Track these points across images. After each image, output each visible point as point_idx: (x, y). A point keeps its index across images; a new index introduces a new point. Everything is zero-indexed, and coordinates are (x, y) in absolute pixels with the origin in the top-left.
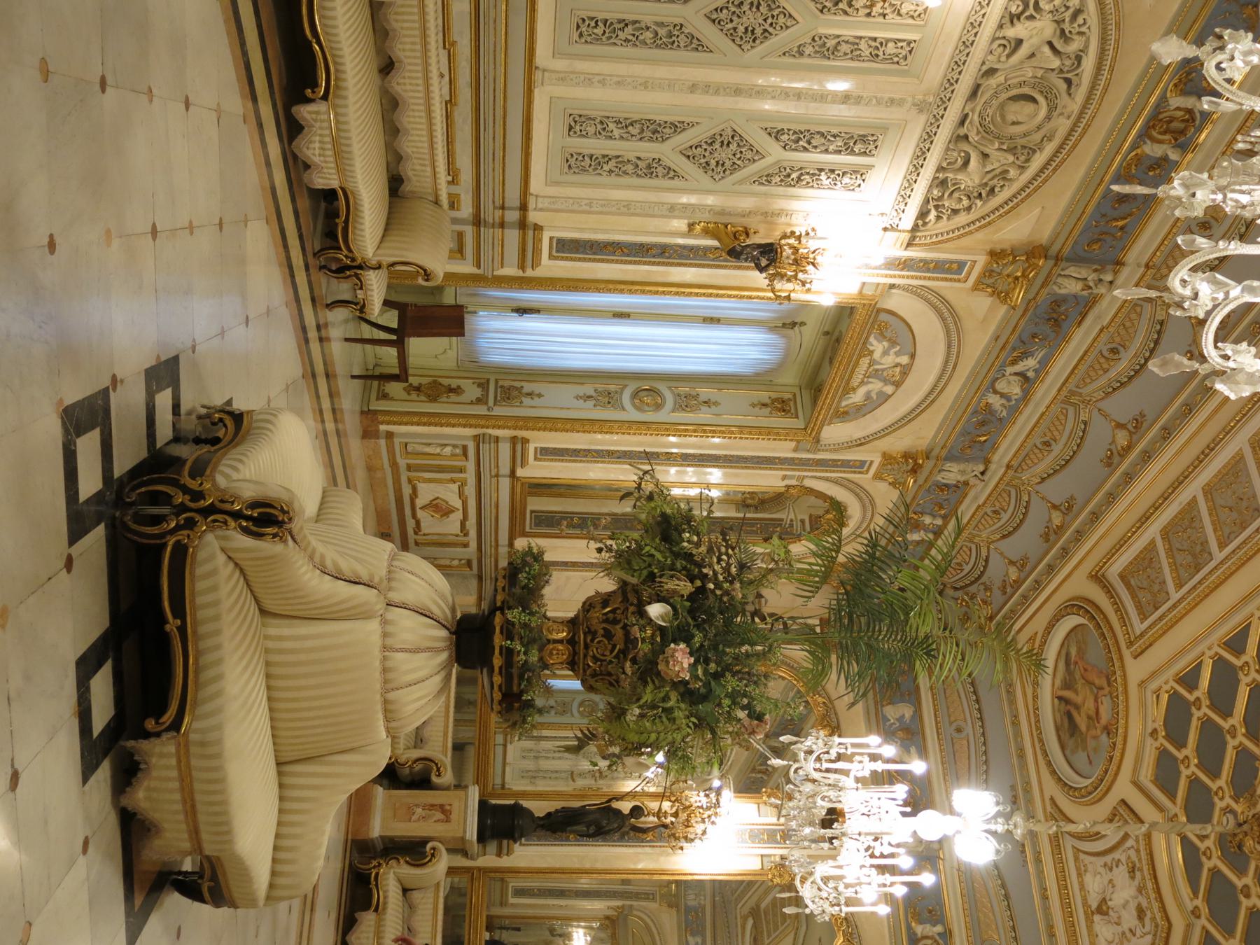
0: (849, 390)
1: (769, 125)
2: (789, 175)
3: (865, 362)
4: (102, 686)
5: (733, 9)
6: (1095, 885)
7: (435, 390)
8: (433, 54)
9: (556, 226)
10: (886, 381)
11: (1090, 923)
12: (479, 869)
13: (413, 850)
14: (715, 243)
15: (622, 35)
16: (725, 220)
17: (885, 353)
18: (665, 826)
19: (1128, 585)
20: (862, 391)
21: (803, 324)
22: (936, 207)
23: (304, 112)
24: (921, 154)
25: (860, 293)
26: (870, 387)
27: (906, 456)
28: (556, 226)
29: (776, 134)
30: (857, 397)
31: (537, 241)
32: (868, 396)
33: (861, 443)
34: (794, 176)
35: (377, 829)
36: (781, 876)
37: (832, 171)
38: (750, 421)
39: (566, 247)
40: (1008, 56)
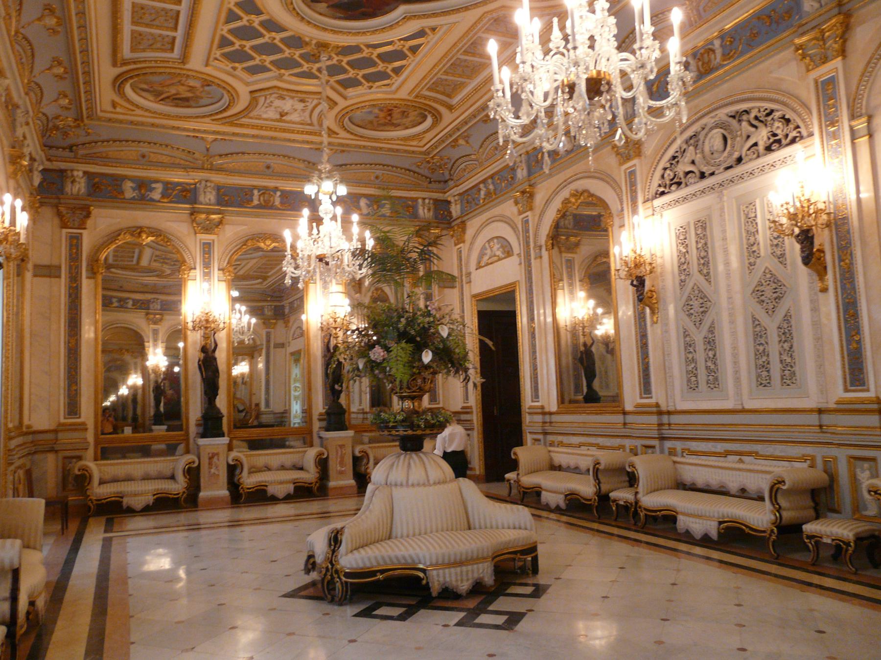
6: (272, 114)
11: (285, 122)
19: (144, 50)
35: (224, 492)
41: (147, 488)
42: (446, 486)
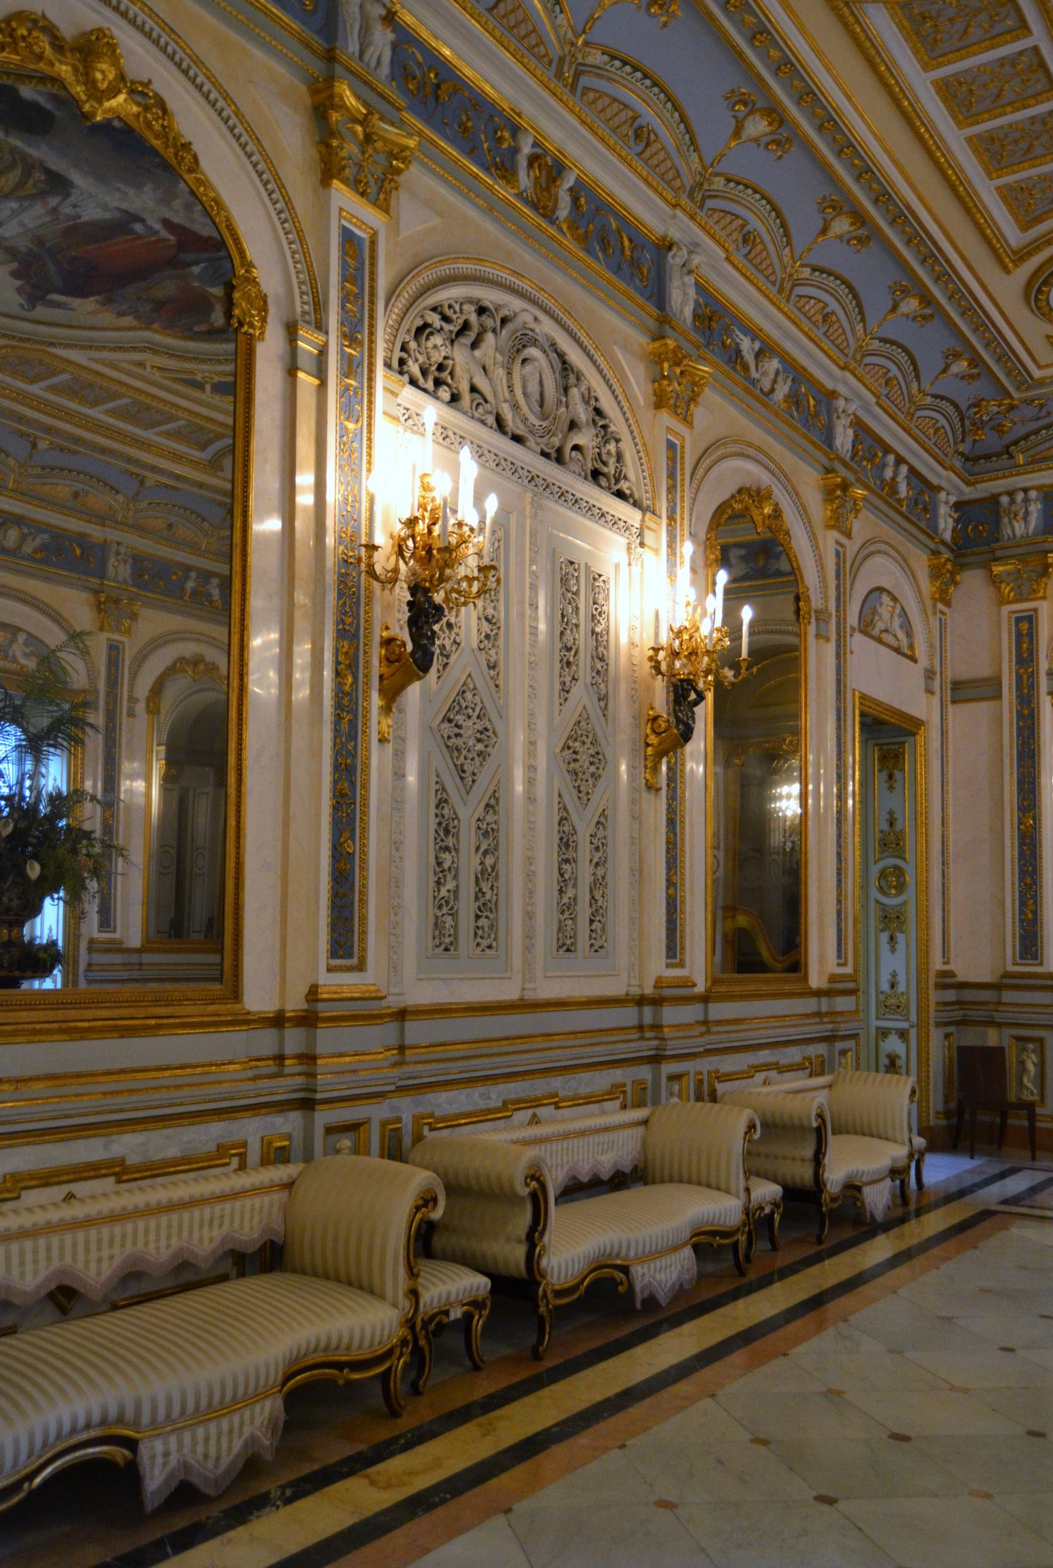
5: (462, 758)
14: (664, 760)
40: (486, 401)
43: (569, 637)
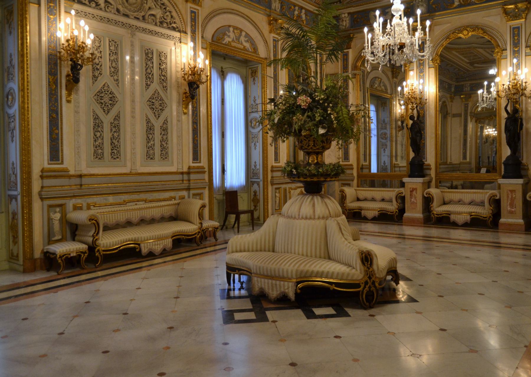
0: (245, 49)
1: (145, 89)
2: (163, 80)
3: (233, 44)
4: (318, 311)
7: (255, 200)
8: (128, 208)
9: (188, 161)
10: (240, 35)
12: (436, 176)
13: (428, 201)
15: (116, 143)
16: (181, 101)
17: (229, 37)
18: (417, 107)
20: (245, 44)
21: (222, 68)
22: (171, 24)
23: (145, 251)
24: (151, 32)
25: (206, 49)
26: (243, 41)
27: (270, 24)
28: (188, 161)
29: (148, 86)
30: (247, 45)
31: (194, 168)
32: (247, 41)
33: (266, 42)
34: (163, 78)
35: (419, 215)
36: (436, 60)
37: (160, 64)
38: (260, 85)
39: (196, 157)
40: (111, 5)
41: (374, 206)
42: (313, 222)
43: (149, 71)
